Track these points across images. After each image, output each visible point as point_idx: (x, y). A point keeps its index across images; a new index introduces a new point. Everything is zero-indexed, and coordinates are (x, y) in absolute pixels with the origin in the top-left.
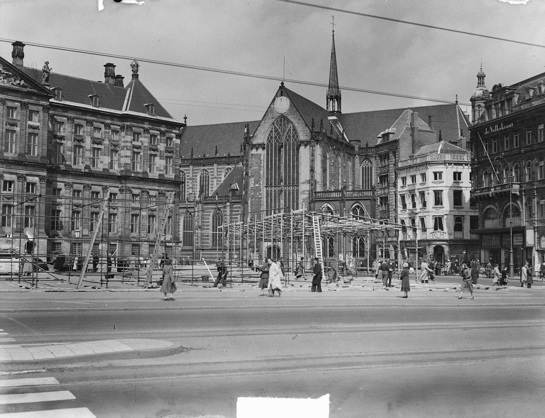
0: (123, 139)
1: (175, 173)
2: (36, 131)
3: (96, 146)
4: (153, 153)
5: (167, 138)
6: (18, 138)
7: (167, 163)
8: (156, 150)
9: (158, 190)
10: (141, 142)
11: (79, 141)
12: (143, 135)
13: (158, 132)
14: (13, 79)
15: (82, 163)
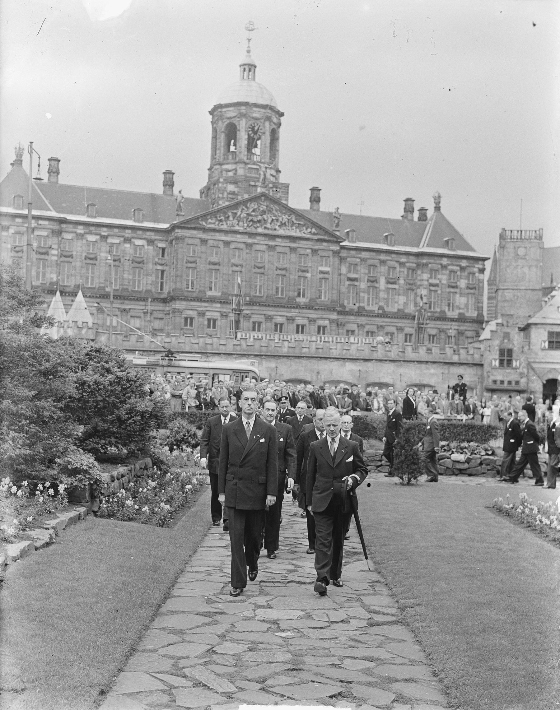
0: (419, 278)
1: (478, 310)
2: (326, 276)
3: (390, 286)
4: (452, 290)
5: (469, 273)
6: (310, 283)
7: (468, 301)
8: (456, 287)
9: (458, 330)
10: (439, 279)
11: (372, 282)
12: (440, 273)
13: (458, 268)
14: (304, 228)
15: (376, 304)
